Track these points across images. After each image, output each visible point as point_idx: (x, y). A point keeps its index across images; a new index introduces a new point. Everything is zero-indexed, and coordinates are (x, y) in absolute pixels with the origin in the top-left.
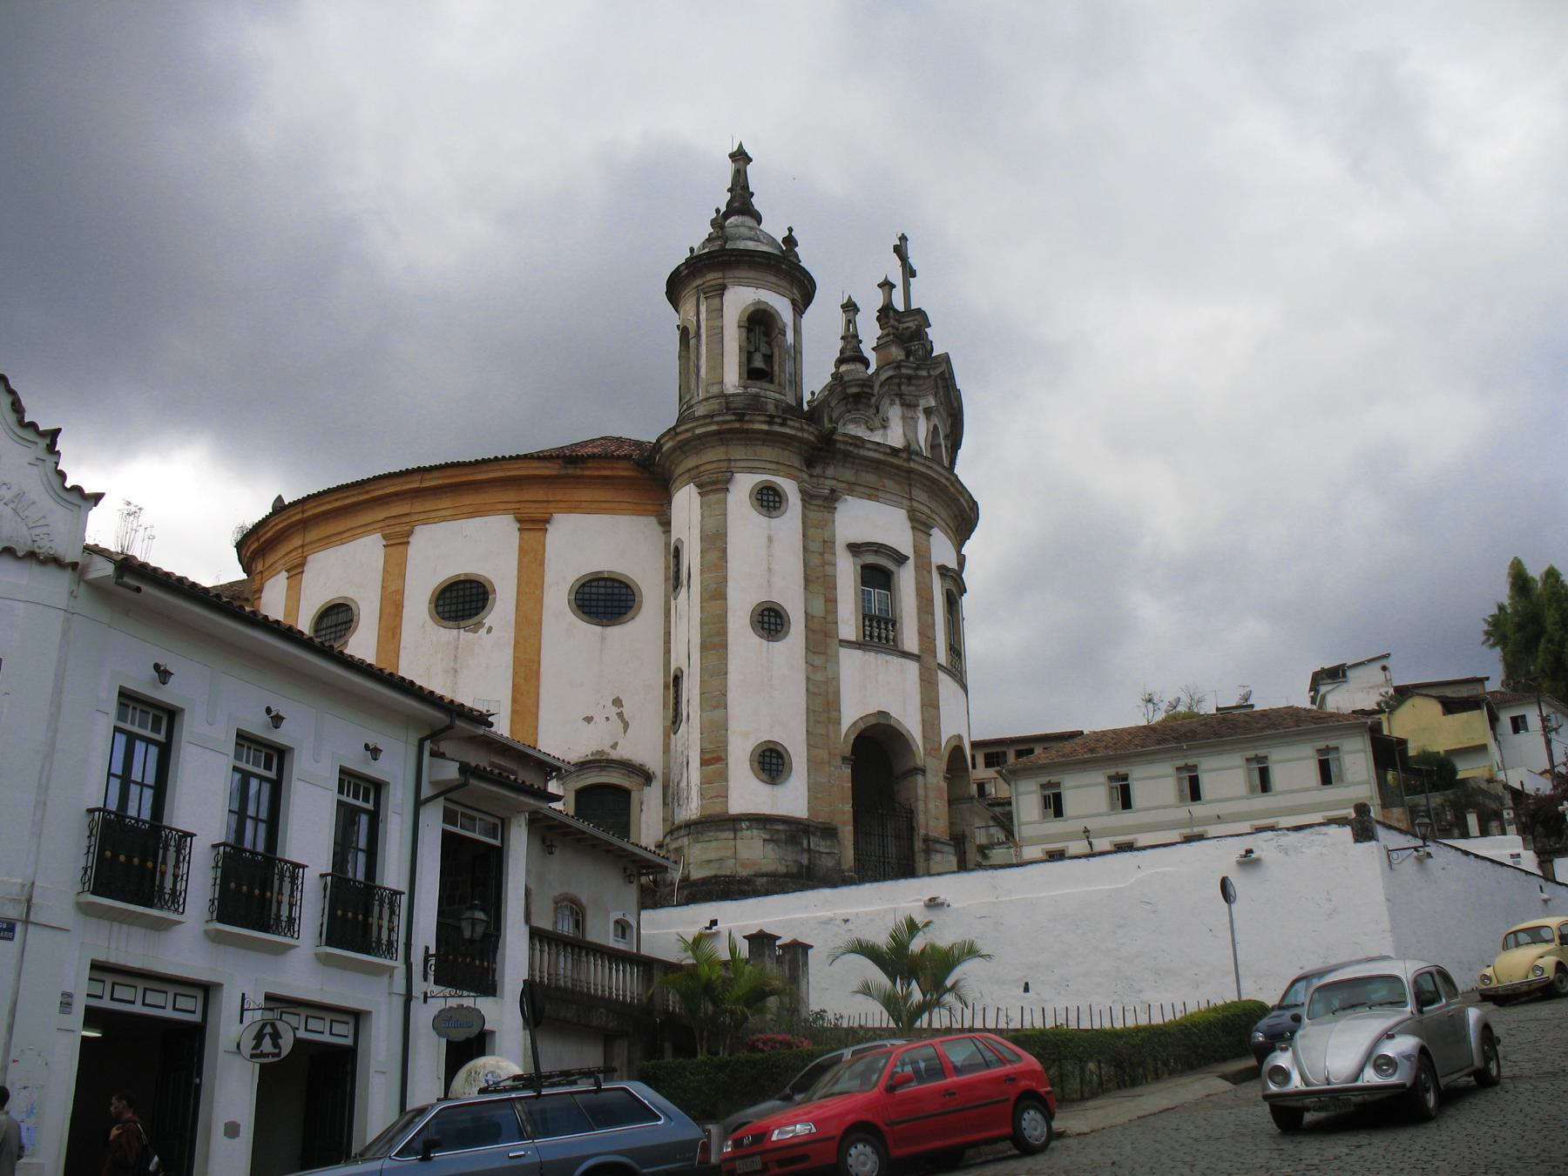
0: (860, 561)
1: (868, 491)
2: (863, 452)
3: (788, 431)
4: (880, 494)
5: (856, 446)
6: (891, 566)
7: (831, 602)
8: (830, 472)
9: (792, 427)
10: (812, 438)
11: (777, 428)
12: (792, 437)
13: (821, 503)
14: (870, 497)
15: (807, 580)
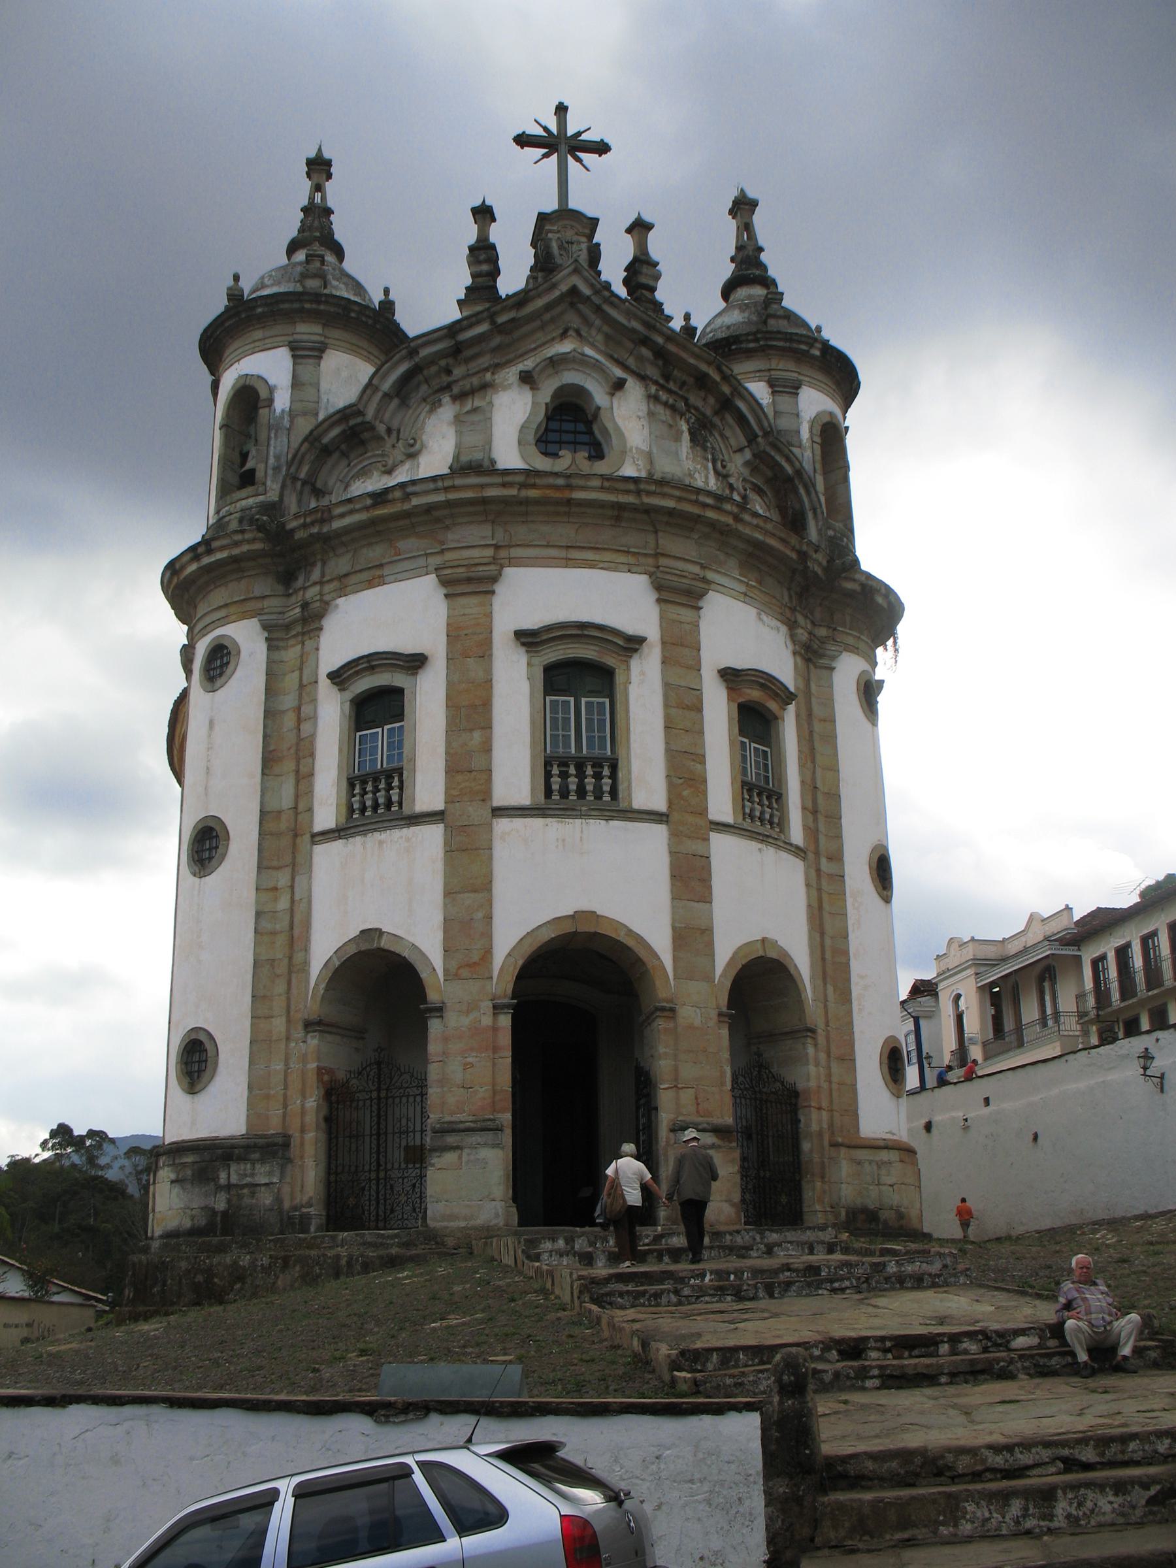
0: (349, 695)
1: (365, 576)
2: (337, 524)
3: (219, 556)
4: (386, 571)
5: (322, 521)
6: (397, 679)
7: (304, 778)
8: (316, 575)
9: (222, 548)
10: (258, 546)
11: (206, 560)
12: (234, 560)
13: (294, 629)
14: (371, 584)
15: (269, 761)
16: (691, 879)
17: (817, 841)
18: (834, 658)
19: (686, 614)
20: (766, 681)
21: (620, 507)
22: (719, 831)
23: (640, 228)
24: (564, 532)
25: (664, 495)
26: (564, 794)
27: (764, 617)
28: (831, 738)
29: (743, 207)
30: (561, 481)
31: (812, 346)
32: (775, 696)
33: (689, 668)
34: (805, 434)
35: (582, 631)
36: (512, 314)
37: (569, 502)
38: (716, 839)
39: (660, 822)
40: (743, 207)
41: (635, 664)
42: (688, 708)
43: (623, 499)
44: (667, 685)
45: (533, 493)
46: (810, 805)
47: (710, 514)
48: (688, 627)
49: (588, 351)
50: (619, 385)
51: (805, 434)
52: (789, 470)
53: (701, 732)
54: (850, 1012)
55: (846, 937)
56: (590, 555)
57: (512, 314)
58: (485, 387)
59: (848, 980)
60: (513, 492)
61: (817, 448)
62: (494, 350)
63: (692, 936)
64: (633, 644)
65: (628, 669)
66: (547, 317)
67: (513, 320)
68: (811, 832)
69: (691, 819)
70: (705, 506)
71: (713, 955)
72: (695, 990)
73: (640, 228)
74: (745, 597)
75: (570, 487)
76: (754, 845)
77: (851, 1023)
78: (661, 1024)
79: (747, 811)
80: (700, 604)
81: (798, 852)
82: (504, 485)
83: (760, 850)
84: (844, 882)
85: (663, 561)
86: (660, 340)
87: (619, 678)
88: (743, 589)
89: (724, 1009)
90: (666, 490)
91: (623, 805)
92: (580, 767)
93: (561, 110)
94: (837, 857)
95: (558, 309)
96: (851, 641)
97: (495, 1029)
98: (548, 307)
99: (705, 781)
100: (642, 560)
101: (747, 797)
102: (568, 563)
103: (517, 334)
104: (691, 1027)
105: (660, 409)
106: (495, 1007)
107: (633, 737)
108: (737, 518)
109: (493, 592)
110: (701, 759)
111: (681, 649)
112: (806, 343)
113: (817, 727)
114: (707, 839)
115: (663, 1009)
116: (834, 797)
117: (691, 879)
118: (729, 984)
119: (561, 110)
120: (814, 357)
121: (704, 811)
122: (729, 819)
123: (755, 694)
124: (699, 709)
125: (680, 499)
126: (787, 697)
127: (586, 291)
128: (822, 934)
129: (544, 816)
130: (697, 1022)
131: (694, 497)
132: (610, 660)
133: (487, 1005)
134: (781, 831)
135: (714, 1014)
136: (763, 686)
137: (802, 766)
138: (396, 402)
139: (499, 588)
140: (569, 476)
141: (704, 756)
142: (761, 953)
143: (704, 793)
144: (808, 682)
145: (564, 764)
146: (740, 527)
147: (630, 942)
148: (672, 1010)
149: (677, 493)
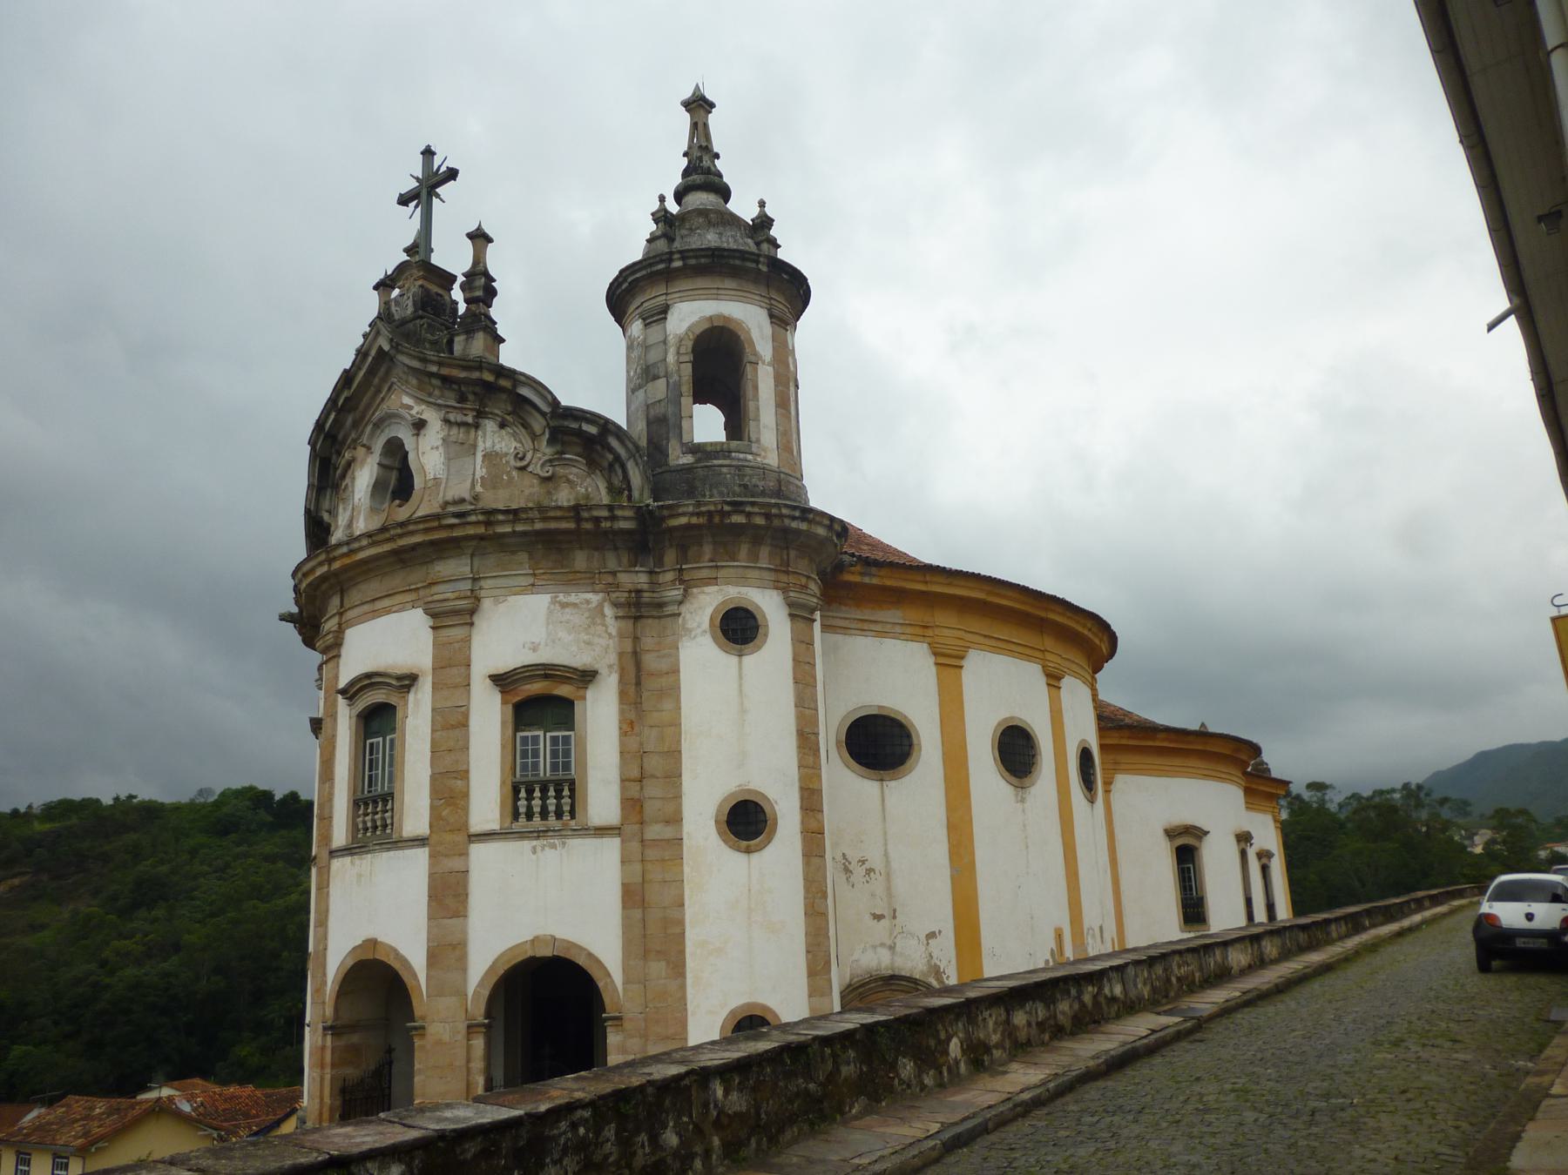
16: (448, 895)
17: (641, 812)
18: (681, 603)
19: (458, 633)
20: (548, 672)
21: (394, 552)
22: (480, 841)
23: (480, 238)
24: (372, 587)
25: (412, 533)
26: (366, 829)
27: (561, 597)
28: (674, 691)
29: (699, 105)
30: (345, 549)
31: (671, 260)
32: (565, 680)
33: (456, 687)
34: (671, 358)
35: (369, 681)
36: (345, 394)
37: (364, 562)
38: (478, 851)
39: (424, 845)
40: (699, 105)
41: (411, 696)
42: (453, 727)
43: (387, 547)
44: (433, 710)
45: (336, 565)
46: (635, 773)
47: (457, 533)
48: (457, 645)
49: (407, 400)
50: (419, 425)
51: (671, 358)
52: (593, 430)
53: (466, 748)
54: (683, 987)
55: (682, 905)
56: (386, 603)
57: (345, 394)
58: (349, 464)
59: (682, 952)
60: (325, 568)
61: (687, 370)
62: (355, 424)
63: (447, 952)
64: (408, 681)
65: (406, 704)
66: (376, 381)
67: (347, 399)
68: (632, 805)
69: (448, 837)
70: (452, 526)
71: (464, 970)
72: (447, 1004)
73: (480, 238)
74: (532, 588)
75: (352, 552)
76: (527, 845)
77: (683, 998)
78: (417, 1042)
79: (522, 810)
80: (475, 618)
81: (602, 831)
82: (321, 564)
83: (534, 851)
84: (681, 845)
85: (435, 589)
86: (434, 369)
87: (399, 714)
88: (531, 580)
89: (481, 1019)
90: (411, 528)
91: (395, 837)
92: (375, 802)
93: (428, 153)
94: (676, 819)
95: (383, 370)
96: (705, 573)
97: (323, 1048)
98: (372, 372)
99: (466, 795)
100: (422, 593)
101: (523, 794)
102: (376, 614)
103: (361, 407)
104: (439, 1042)
105: (454, 431)
106: (325, 1029)
107: (407, 768)
108: (488, 524)
109: (338, 656)
110: (464, 775)
111: (452, 666)
112: (661, 261)
113: (650, 684)
114: (465, 854)
115: (416, 1028)
116: (675, 754)
117: (448, 895)
118: (486, 993)
119: (428, 153)
120: (678, 269)
121: (466, 824)
122: (496, 826)
123: (536, 688)
124: (464, 724)
125: (427, 530)
126: (587, 677)
127: (386, 348)
128: (644, 908)
129: (352, 854)
130: (446, 1038)
131: (436, 524)
132: (393, 700)
133: (320, 1026)
134: (573, 816)
135: (462, 1027)
136: (546, 676)
137: (623, 734)
138: (329, 492)
139: (344, 651)
140: (347, 543)
141: (467, 771)
142: (530, 953)
143: (466, 810)
144: (636, 639)
145: (366, 805)
146: (500, 529)
147: (397, 966)
148: (423, 1028)
149: (421, 526)
